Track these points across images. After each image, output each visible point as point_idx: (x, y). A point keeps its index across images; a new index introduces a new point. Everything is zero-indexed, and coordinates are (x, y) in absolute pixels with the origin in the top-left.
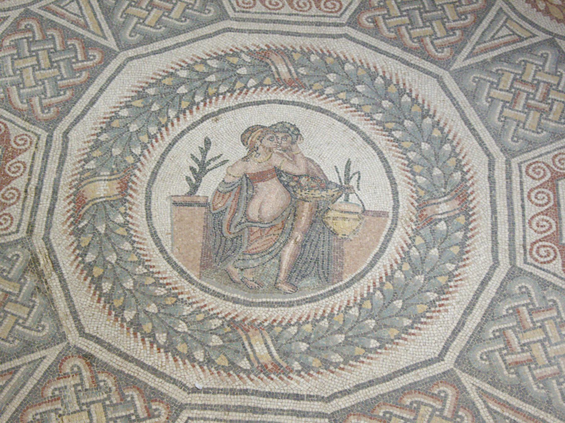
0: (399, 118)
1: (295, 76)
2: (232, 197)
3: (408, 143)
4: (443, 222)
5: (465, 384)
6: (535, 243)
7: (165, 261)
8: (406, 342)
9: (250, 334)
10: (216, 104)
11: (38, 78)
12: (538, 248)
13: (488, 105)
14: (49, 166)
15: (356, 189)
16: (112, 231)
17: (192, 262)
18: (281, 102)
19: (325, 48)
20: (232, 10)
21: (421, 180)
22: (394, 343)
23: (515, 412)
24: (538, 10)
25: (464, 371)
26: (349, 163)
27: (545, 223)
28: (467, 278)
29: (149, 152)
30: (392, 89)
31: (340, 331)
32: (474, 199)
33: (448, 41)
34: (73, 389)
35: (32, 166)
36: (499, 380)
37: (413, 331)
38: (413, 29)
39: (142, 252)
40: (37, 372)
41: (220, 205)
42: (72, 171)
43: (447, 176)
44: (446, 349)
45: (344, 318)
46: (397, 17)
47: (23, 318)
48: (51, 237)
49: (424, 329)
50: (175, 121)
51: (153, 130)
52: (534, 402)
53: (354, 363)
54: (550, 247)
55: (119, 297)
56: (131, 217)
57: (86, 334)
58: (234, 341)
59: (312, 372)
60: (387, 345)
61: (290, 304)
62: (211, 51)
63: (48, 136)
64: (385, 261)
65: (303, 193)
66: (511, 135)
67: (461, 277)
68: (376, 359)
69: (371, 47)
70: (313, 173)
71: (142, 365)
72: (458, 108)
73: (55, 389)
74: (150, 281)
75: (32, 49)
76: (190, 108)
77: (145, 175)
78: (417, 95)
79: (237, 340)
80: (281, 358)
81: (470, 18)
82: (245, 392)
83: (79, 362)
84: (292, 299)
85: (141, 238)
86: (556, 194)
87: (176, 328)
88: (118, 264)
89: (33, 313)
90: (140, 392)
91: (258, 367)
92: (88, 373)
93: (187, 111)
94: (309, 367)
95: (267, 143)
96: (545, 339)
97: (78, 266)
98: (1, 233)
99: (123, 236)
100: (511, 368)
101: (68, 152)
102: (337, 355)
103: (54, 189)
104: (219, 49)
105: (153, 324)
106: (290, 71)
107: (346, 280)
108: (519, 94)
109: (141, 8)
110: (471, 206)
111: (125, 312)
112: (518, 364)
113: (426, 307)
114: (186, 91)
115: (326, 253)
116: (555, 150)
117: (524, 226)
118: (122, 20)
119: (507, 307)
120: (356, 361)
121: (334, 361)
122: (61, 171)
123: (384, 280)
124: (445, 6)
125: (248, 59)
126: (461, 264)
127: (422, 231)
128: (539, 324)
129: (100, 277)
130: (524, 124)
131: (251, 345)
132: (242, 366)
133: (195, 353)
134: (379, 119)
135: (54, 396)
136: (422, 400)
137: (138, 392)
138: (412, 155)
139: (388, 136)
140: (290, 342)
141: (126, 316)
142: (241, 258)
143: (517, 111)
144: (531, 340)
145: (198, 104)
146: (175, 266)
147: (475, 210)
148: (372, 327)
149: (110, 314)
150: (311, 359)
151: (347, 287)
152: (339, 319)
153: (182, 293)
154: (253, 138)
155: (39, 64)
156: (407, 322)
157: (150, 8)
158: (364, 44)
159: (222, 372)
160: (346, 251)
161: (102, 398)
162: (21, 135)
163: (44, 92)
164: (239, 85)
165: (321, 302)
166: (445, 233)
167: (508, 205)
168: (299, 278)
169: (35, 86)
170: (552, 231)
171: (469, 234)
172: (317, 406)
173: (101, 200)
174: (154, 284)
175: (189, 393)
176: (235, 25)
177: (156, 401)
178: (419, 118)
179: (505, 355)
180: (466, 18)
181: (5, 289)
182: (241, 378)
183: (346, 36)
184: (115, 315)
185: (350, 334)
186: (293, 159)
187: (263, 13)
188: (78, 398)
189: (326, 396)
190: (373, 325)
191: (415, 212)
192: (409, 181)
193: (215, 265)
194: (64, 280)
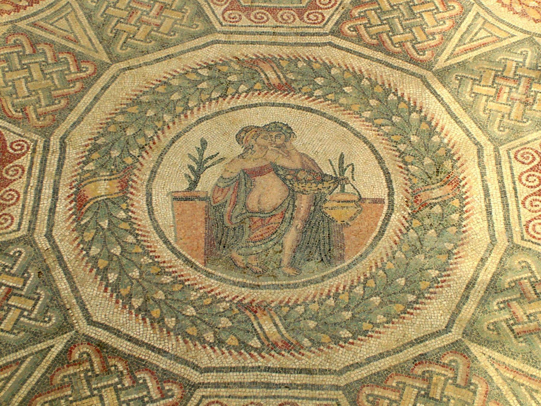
0: (387, 115)
1: (284, 81)
3: (398, 137)
4: (438, 206)
5: (475, 353)
6: (530, 221)
7: (169, 251)
8: (412, 316)
11: (31, 89)
12: (534, 226)
14: (47, 169)
15: (350, 179)
19: (311, 55)
20: (219, 25)
23: (530, 379)
25: (473, 341)
26: (342, 157)
30: (378, 90)
31: (347, 308)
32: (466, 184)
33: (429, 44)
35: (31, 168)
37: (418, 306)
38: (394, 35)
39: (146, 244)
41: (219, 199)
45: (349, 296)
46: (378, 25)
47: (28, 311)
48: (54, 233)
51: (150, 133)
55: (126, 287)
56: (133, 212)
57: (95, 322)
59: (322, 347)
60: (393, 320)
61: (296, 286)
62: (201, 61)
63: (45, 141)
65: (300, 186)
66: (496, 125)
67: (461, 254)
68: (383, 333)
69: (355, 53)
70: (308, 167)
71: (153, 348)
73: (65, 376)
75: (23, 62)
79: (246, 321)
81: (449, 23)
84: (297, 281)
85: (144, 231)
87: (184, 312)
88: (123, 256)
89: (38, 305)
91: (268, 345)
92: (98, 359)
94: (318, 343)
95: (260, 141)
98: (1, 232)
99: (127, 230)
100: (520, 337)
104: (208, 59)
105: (161, 310)
106: (279, 77)
107: (349, 261)
109: (131, 25)
110: (464, 190)
111: (133, 299)
114: (180, 98)
117: (518, 206)
120: (366, 336)
121: (343, 336)
122: (61, 173)
123: (385, 261)
124: (423, 14)
125: (237, 67)
126: (459, 243)
129: (106, 269)
132: (252, 345)
133: (204, 335)
134: (368, 116)
135: (64, 383)
137: (150, 374)
138: (402, 147)
141: (134, 304)
142: (244, 245)
145: (192, 110)
146: (179, 255)
147: (467, 194)
148: (377, 304)
149: (117, 302)
152: (345, 297)
153: (188, 280)
154: (247, 137)
156: (411, 298)
157: (138, 24)
158: (348, 50)
159: (233, 351)
161: (113, 382)
164: (231, 90)
165: (325, 283)
168: (302, 261)
169: (28, 96)
171: (465, 216)
172: (330, 380)
173: (102, 198)
175: (201, 373)
176: (223, 38)
177: (169, 381)
179: (513, 325)
180: (444, 22)
181: (8, 283)
182: (252, 356)
183: (330, 44)
185: (356, 310)
189: (338, 369)
190: (379, 301)
193: (219, 253)
194: (69, 273)
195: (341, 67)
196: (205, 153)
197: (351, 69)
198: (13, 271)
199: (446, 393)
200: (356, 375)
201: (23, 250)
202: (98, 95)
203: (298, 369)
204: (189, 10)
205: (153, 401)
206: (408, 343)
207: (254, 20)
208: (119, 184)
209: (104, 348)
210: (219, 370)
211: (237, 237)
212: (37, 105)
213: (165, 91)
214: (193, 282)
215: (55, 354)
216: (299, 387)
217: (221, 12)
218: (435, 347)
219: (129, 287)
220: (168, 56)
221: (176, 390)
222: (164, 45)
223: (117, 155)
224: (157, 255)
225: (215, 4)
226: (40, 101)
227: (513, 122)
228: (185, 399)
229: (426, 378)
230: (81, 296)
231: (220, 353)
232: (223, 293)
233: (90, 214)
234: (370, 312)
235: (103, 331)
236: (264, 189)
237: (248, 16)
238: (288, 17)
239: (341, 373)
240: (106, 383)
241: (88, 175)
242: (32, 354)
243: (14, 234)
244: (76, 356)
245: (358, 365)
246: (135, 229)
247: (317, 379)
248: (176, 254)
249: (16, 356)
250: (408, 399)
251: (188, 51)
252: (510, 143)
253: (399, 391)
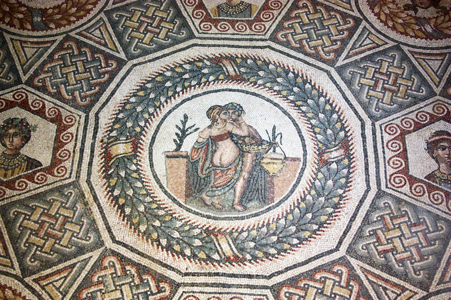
1: (238, 73)
2: (203, 151)
4: (334, 163)
5: (353, 265)
6: (392, 175)
9: (218, 238)
10: (190, 93)
12: (394, 178)
13: (359, 88)
14: (87, 135)
15: (279, 144)
16: (129, 175)
18: (230, 90)
19: (256, 55)
21: (320, 137)
24: (389, 27)
25: (352, 257)
26: (274, 128)
27: (398, 162)
28: (351, 198)
29: (150, 125)
30: (299, 80)
31: (274, 234)
34: (110, 276)
35: (77, 136)
36: (374, 262)
38: (310, 41)
39: (148, 188)
40: (87, 266)
43: (336, 134)
44: (340, 243)
47: (77, 233)
48: (91, 180)
49: (326, 231)
50: (165, 104)
51: (151, 110)
52: (397, 275)
54: (402, 177)
55: (136, 218)
56: (141, 166)
59: (258, 260)
61: (243, 218)
64: (300, 189)
66: (374, 107)
68: (297, 251)
71: (153, 260)
72: (341, 91)
73: (99, 277)
74: (154, 206)
76: (174, 96)
77: (148, 139)
78: (315, 84)
79: (211, 242)
82: (217, 274)
83: (113, 259)
84: (244, 215)
86: (404, 144)
89: (83, 229)
90: (153, 277)
93: (172, 98)
95: (223, 116)
96: (401, 236)
97: (109, 198)
99: (136, 178)
101: (99, 126)
104: (190, 57)
106: (235, 70)
107: (276, 202)
110: (352, 153)
112: (385, 251)
113: (327, 217)
115: (263, 185)
116: (402, 116)
117: (385, 164)
118: (128, 40)
119: (377, 215)
122: (96, 138)
123: (300, 201)
124: (330, 27)
125: (208, 63)
126: (347, 189)
127: (321, 170)
128: (397, 226)
129: (124, 205)
130: (382, 100)
131: (219, 244)
134: (292, 99)
136: (327, 276)
138: (313, 122)
140: (243, 242)
144: (393, 236)
145: (179, 93)
146: (170, 196)
147: (354, 155)
149: (131, 228)
150: (257, 252)
151: (277, 206)
152: (273, 226)
153: (175, 213)
155: (77, 70)
156: (315, 227)
158: (281, 52)
159: (202, 262)
160: (275, 183)
161: (129, 281)
163: (82, 88)
164: (204, 80)
165: (261, 216)
166: (336, 170)
167: (375, 152)
169: (76, 84)
170: (402, 167)
171: (351, 171)
172: (262, 282)
174: (157, 208)
176: (199, 42)
177: (162, 282)
178: (317, 98)
179: (377, 246)
180: (344, 33)
182: (214, 266)
184: (134, 229)
185: (281, 235)
187: (216, 34)
188: (114, 282)
189: (267, 275)
190: (295, 229)
191: (317, 157)
194: (101, 207)
195: (275, 63)
198: (67, 206)
205: (152, 294)
217: (198, 24)
221: (168, 288)
222: (161, 47)
225: (194, 17)
228: (174, 292)
237: (216, 26)
238: (242, 27)
243: (67, 180)
244: (106, 263)
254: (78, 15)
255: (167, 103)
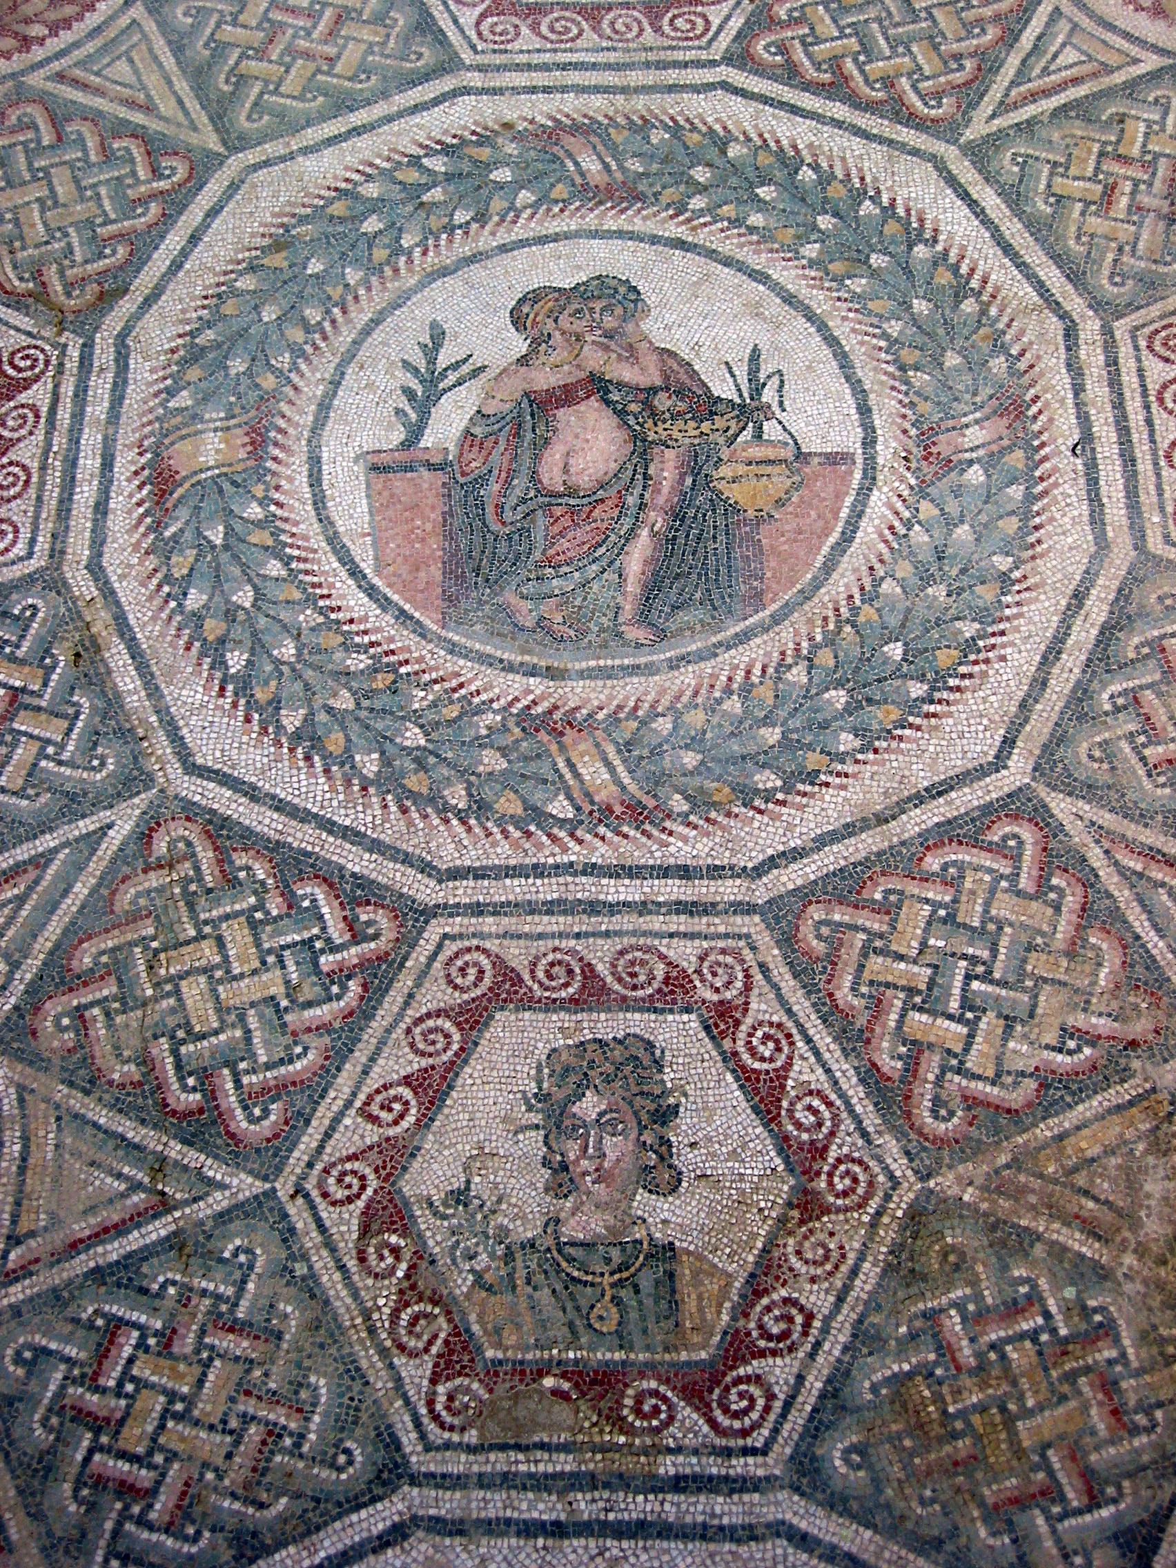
0: (858, 251)
1: (619, 176)
5: (1060, 816)
7: (361, 595)
14: (89, 409)
15: (775, 407)
17: (422, 591)
19: (681, 113)
22: (893, 738)
28: (1042, 584)
31: (767, 721)
32: (1040, 412)
33: (949, 82)
35: (53, 410)
37: (932, 708)
38: (870, 61)
39: (308, 578)
41: (473, 465)
42: (140, 416)
44: (1009, 743)
45: (777, 690)
47: (55, 744)
50: (362, 292)
53: (808, 788)
55: (266, 683)
56: (279, 505)
57: (199, 767)
58: (531, 759)
59: (713, 815)
60: (877, 743)
61: (650, 670)
62: (429, 138)
63: (84, 345)
66: (1106, 272)
68: (855, 776)
69: (782, 105)
71: (328, 826)
72: (986, 222)
75: (36, 165)
79: (538, 756)
80: (641, 788)
81: (992, 33)
84: (655, 657)
85: (306, 549)
88: (259, 609)
90: (331, 885)
91: (591, 813)
92: (211, 854)
99: (267, 548)
100: (1158, 775)
102: (767, 772)
103: (103, 456)
106: (606, 167)
108: (1116, 183)
109: (271, 62)
110: (1036, 427)
111: (283, 712)
114: (381, 226)
117: (1156, 464)
119: (1136, 640)
120: (812, 784)
121: (760, 786)
122: (118, 417)
123: (858, 603)
124: (935, 12)
125: (511, 149)
129: (222, 641)
131: (571, 765)
132: (554, 812)
133: (446, 793)
134: (814, 255)
137: (325, 887)
139: (838, 290)
141: (285, 722)
143: (1115, 220)
145: (409, 254)
146: (384, 603)
147: (1044, 438)
149: (248, 720)
152: (765, 693)
153: (407, 662)
156: (917, 690)
158: (765, 100)
159: (511, 828)
161: (245, 905)
162: (24, 348)
164: (497, 204)
165: (720, 659)
167: (1117, 423)
169: (47, 243)
172: (729, 890)
173: (209, 473)
175: (440, 882)
176: (475, 79)
177: (368, 903)
179: (1144, 746)
180: (983, 30)
181: (11, 682)
183: (725, 86)
185: (791, 724)
186: (631, 353)
189: (750, 865)
190: (843, 700)
192: (892, 382)
195: (749, 139)
196: (440, 357)
197: (772, 144)
198: (20, 653)
199: (994, 912)
200: (791, 877)
201: (40, 603)
202: (196, 230)
203: (660, 867)
204: (401, 19)
206: (909, 799)
207: (550, 35)
208: (247, 440)
209: (222, 827)
210: (479, 874)
211: (518, 557)
212: (67, 262)
213: (348, 213)
214: (417, 667)
215: (117, 842)
216: (663, 910)
217: (473, 21)
218: (970, 806)
219: (273, 683)
220: (354, 129)
222: (343, 104)
223: (242, 369)
224: (334, 604)
226: (71, 253)
227: (1143, 264)
228: (408, 942)
229: (951, 879)
230: (168, 708)
231: (482, 835)
232: (486, 690)
233: (183, 513)
234: (824, 726)
235: (217, 789)
236: (577, 436)
237: (535, 28)
239: (759, 871)
240: (228, 909)
241: (179, 419)
242: (66, 844)
244: (161, 847)
245: (796, 854)
246: (285, 545)
247: (704, 890)
248: (377, 601)
249: (35, 847)
250: (909, 929)
251: (400, 115)
252: (1138, 314)
253: (888, 913)
254: (52, 16)
255: (369, 289)
